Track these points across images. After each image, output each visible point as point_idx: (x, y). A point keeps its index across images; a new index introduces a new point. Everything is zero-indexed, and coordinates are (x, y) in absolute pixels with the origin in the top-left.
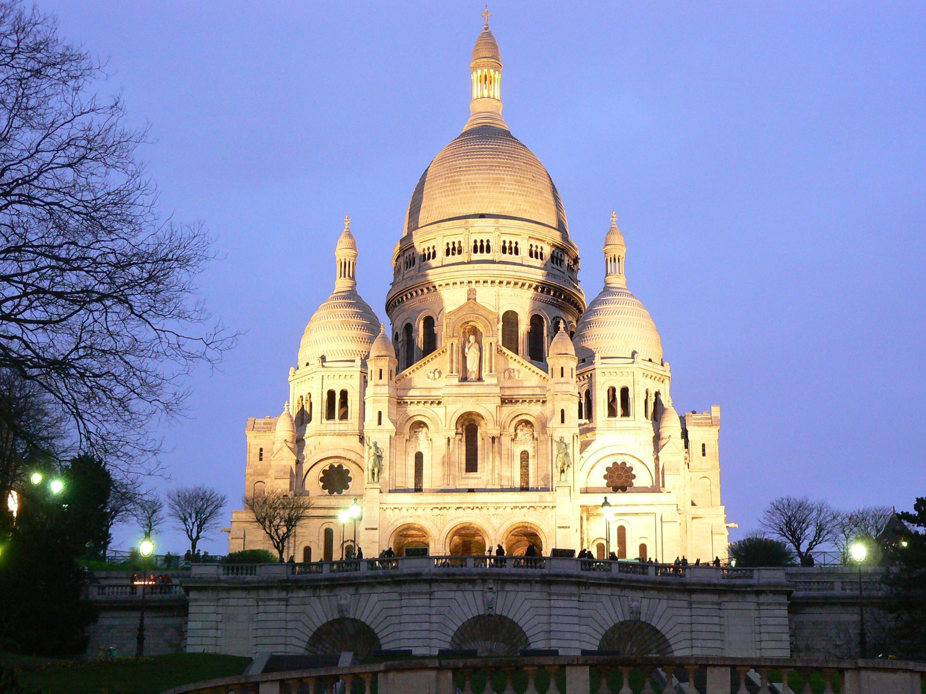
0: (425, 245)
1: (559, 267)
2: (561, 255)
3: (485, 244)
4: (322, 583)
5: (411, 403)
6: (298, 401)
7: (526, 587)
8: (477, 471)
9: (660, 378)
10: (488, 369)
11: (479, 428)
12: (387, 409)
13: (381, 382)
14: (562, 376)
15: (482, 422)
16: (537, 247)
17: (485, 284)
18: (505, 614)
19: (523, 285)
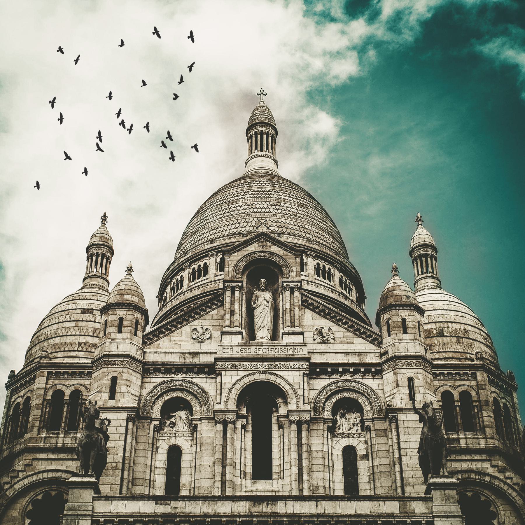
8: (270, 478)
13: (119, 336)
16: (324, 266)
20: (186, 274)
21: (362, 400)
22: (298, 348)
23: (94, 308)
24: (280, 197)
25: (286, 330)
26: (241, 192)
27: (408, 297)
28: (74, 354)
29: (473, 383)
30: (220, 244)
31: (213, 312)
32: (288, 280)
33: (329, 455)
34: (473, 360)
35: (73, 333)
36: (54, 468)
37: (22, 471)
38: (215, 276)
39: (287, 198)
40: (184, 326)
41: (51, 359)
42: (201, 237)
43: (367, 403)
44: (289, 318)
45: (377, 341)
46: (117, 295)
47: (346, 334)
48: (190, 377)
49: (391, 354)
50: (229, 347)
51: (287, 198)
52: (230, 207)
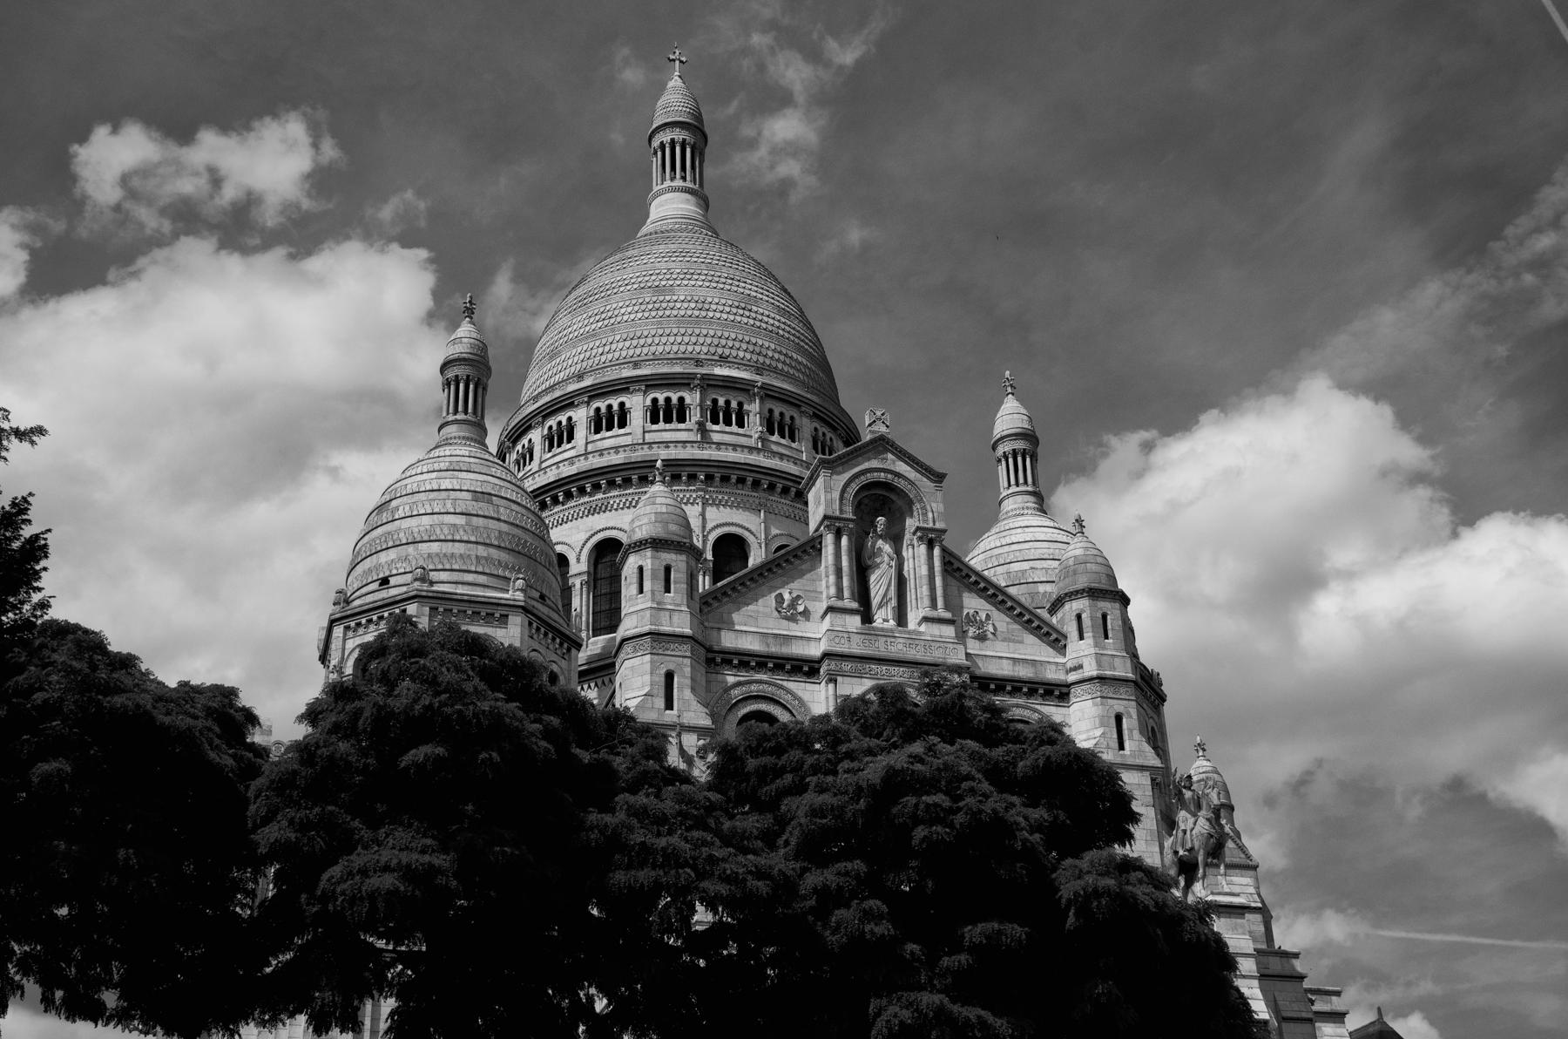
12: (688, 670)
16: (824, 434)
17: (740, 486)
20: (581, 415)
22: (951, 646)
25: (929, 613)
26: (678, 271)
28: (470, 578)
30: (654, 372)
31: (803, 567)
32: (926, 526)
35: (465, 538)
38: (644, 432)
40: (760, 585)
41: (432, 583)
42: (607, 349)
45: (1057, 641)
46: (656, 522)
47: (1010, 626)
48: (779, 679)
50: (846, 635)
51: (761, 296)
52: (661, 298)
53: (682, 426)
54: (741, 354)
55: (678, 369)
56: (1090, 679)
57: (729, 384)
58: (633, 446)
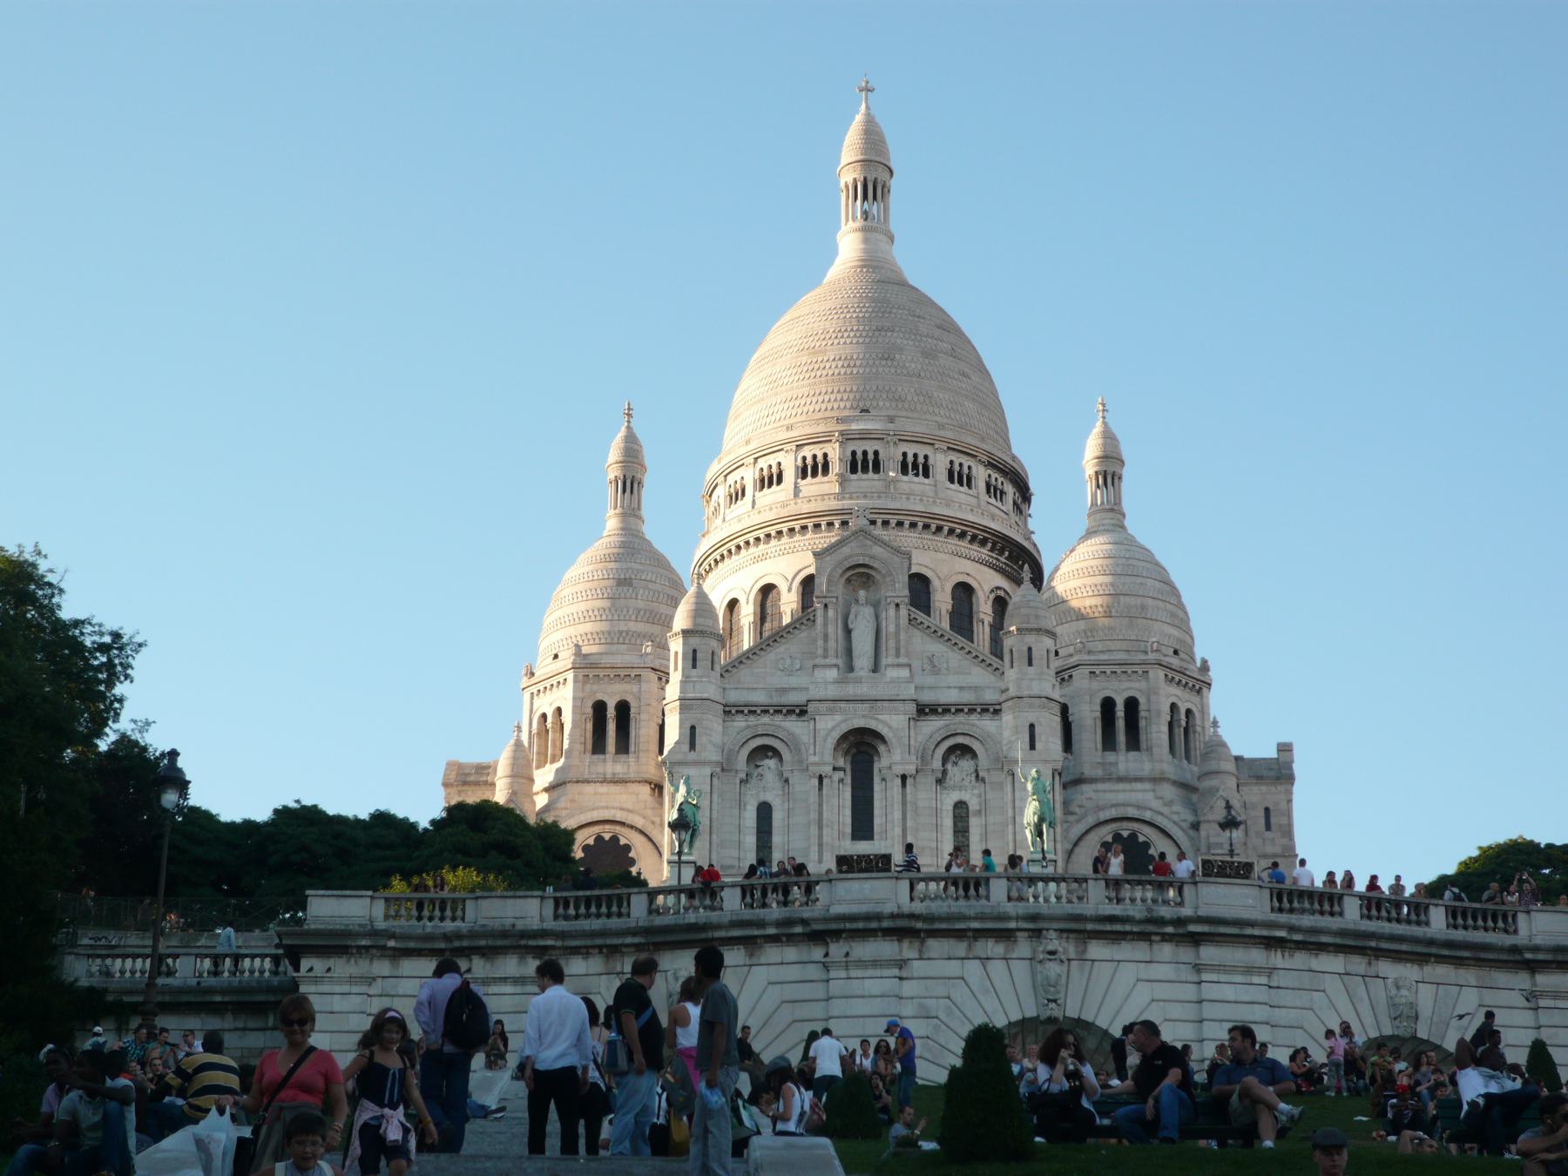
0: (763, 463)
1: (999, 504)
2: (1002, 483)
3: (871, 457)
4: (629, 940)
5: (750, 712)
6: (539, 723)
7: (1139, 950)
9: (1194, 686)
10: (892, 652)
11: (876, 758)
14: (1030, 664)
15: (882, 748)
16: (961, 465)
18: (1088, 1016)
19: (939, 529)
21: (976, 746)
23: (633, 577)
24: (893, 341)
27: (1037, 617)
29: (1143, 685)
30: (803, 433)
31: (802, 635)
33: (937, 812)
34: (1146, 653)
36: (604, 804)
37: (566, 809)
39: (906, 342)
43: (983, 750)
44: (894, 645)
49: (1012, 692)
53: (826, 479)
54: (881, 404)
55: (821, 428)
56: (1012, 698)
57: (864, 436)
58: (784, 505)
